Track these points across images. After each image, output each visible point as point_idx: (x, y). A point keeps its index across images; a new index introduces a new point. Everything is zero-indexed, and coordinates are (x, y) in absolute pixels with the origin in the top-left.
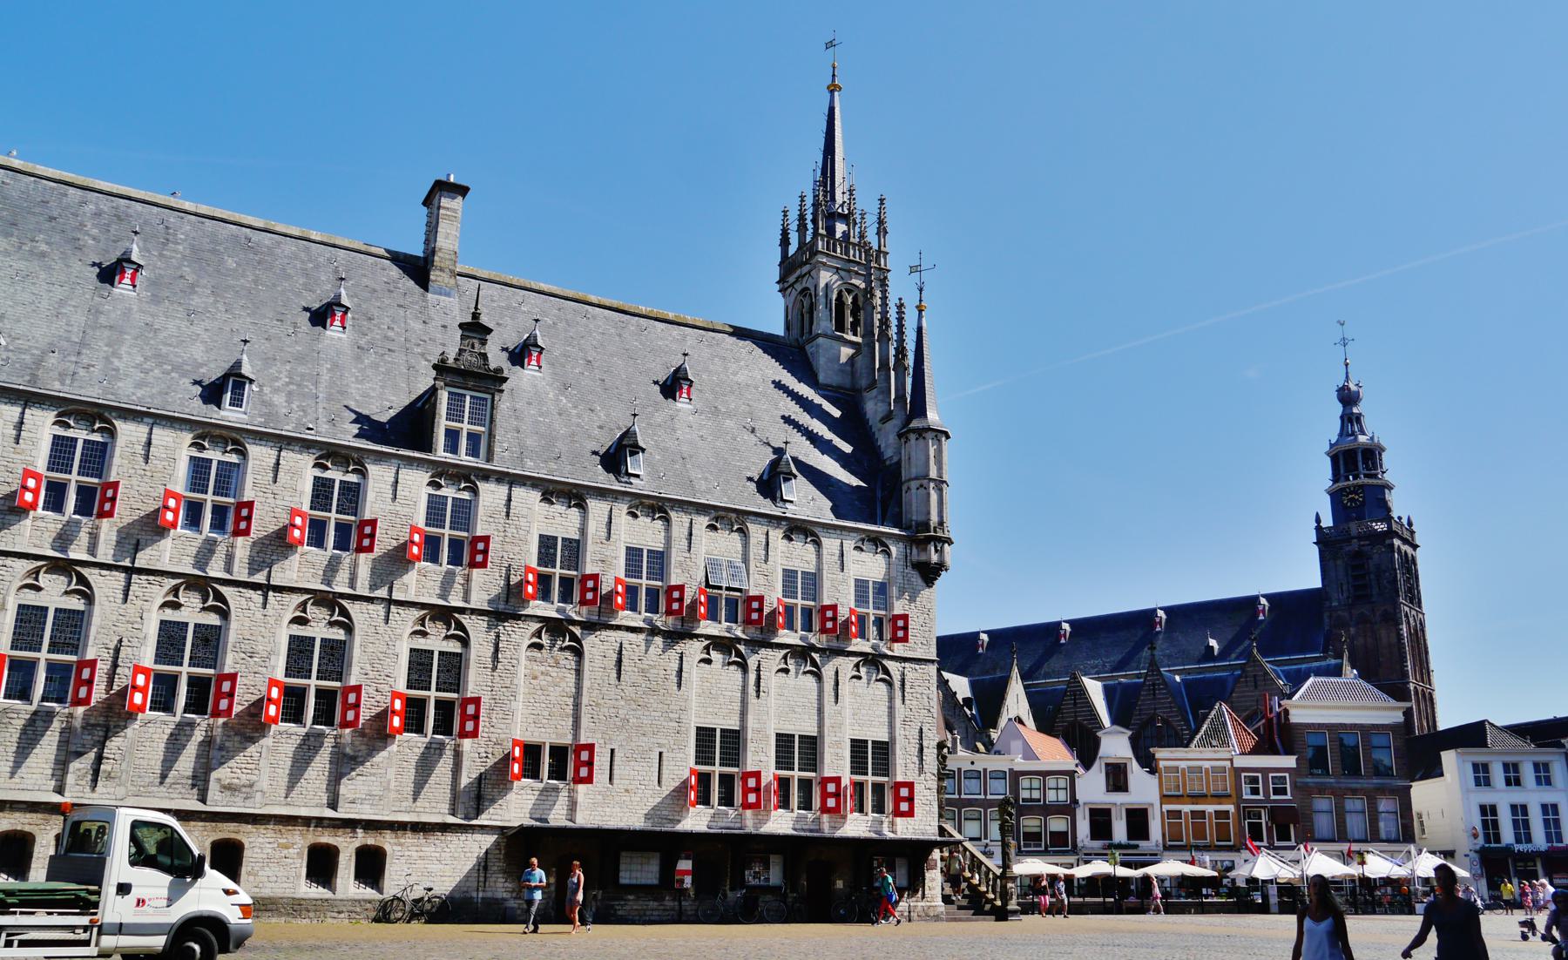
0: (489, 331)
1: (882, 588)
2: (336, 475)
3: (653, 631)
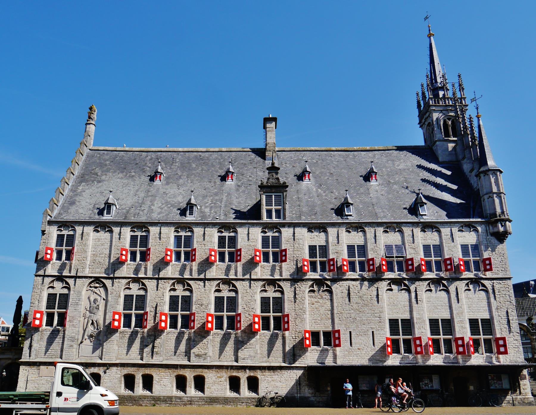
0: (279, 169)
1: (476, 247)
2: (226, 234)
3: (363, 279)
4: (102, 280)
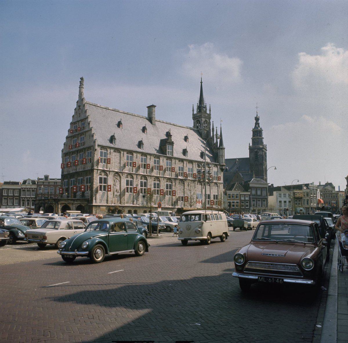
4: (119, 173)
